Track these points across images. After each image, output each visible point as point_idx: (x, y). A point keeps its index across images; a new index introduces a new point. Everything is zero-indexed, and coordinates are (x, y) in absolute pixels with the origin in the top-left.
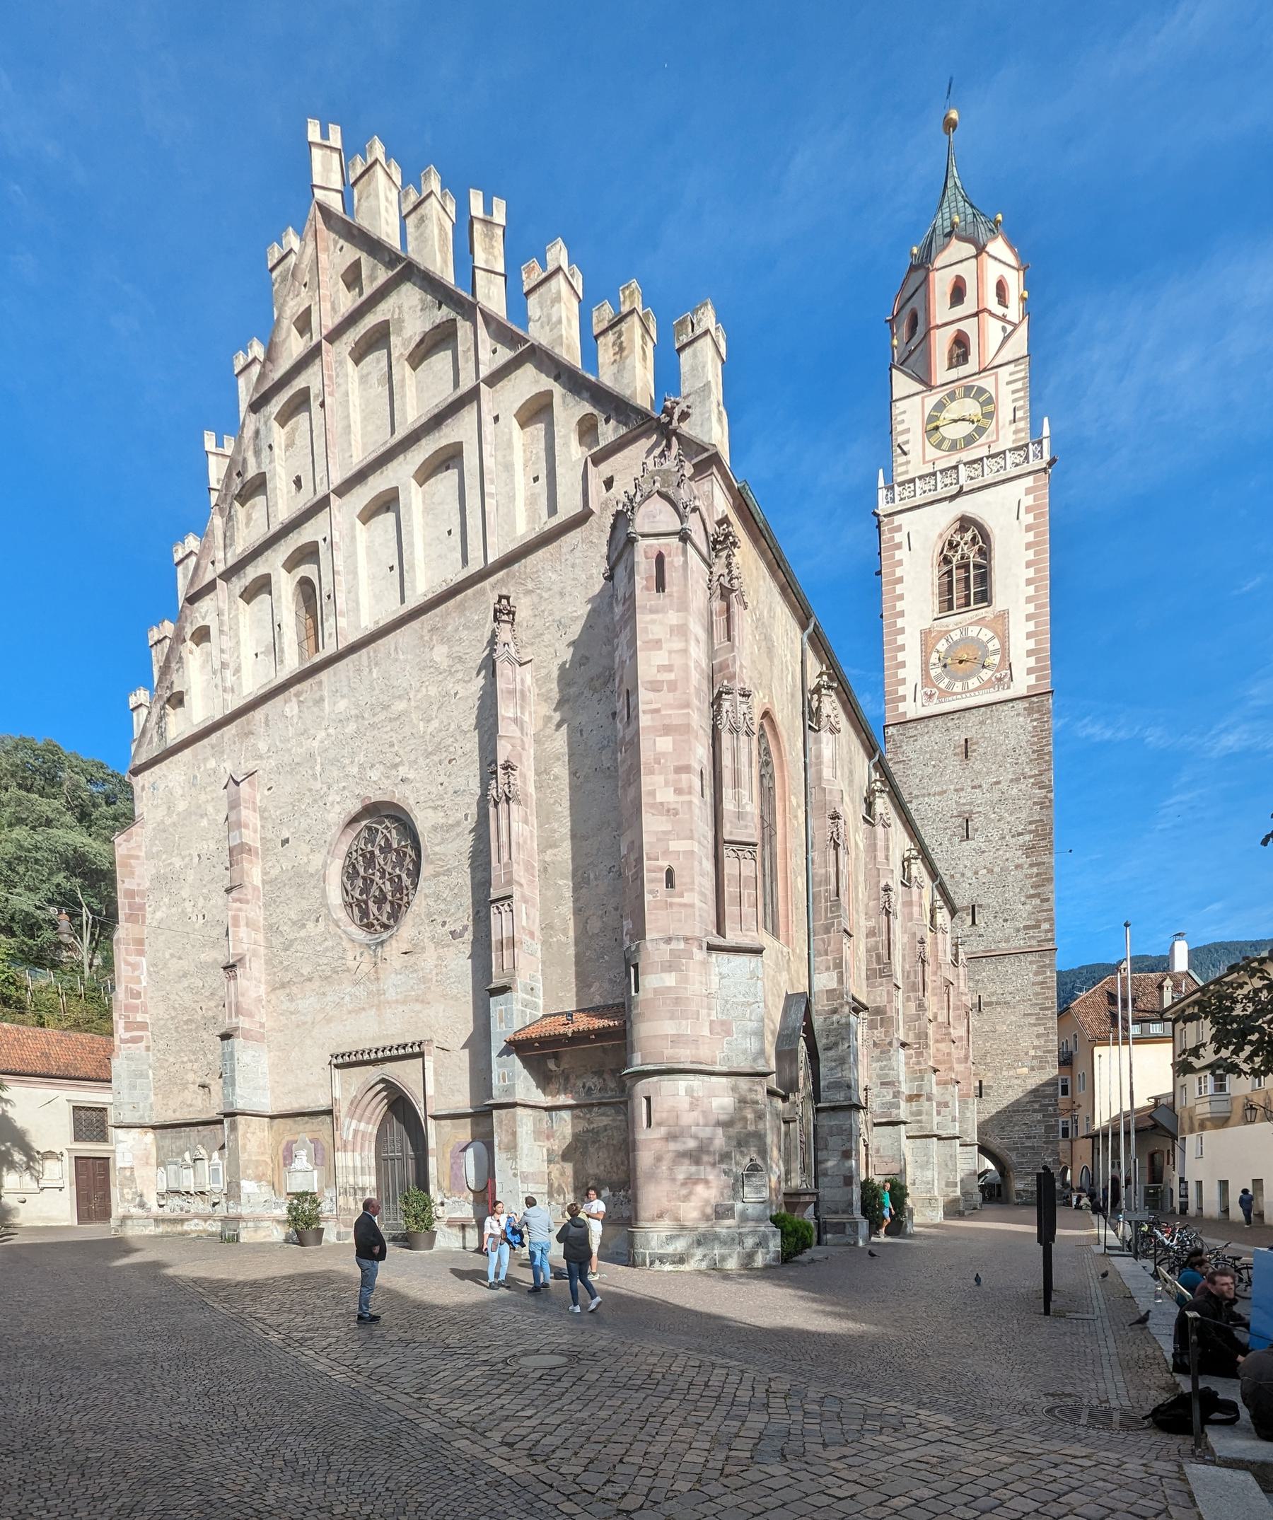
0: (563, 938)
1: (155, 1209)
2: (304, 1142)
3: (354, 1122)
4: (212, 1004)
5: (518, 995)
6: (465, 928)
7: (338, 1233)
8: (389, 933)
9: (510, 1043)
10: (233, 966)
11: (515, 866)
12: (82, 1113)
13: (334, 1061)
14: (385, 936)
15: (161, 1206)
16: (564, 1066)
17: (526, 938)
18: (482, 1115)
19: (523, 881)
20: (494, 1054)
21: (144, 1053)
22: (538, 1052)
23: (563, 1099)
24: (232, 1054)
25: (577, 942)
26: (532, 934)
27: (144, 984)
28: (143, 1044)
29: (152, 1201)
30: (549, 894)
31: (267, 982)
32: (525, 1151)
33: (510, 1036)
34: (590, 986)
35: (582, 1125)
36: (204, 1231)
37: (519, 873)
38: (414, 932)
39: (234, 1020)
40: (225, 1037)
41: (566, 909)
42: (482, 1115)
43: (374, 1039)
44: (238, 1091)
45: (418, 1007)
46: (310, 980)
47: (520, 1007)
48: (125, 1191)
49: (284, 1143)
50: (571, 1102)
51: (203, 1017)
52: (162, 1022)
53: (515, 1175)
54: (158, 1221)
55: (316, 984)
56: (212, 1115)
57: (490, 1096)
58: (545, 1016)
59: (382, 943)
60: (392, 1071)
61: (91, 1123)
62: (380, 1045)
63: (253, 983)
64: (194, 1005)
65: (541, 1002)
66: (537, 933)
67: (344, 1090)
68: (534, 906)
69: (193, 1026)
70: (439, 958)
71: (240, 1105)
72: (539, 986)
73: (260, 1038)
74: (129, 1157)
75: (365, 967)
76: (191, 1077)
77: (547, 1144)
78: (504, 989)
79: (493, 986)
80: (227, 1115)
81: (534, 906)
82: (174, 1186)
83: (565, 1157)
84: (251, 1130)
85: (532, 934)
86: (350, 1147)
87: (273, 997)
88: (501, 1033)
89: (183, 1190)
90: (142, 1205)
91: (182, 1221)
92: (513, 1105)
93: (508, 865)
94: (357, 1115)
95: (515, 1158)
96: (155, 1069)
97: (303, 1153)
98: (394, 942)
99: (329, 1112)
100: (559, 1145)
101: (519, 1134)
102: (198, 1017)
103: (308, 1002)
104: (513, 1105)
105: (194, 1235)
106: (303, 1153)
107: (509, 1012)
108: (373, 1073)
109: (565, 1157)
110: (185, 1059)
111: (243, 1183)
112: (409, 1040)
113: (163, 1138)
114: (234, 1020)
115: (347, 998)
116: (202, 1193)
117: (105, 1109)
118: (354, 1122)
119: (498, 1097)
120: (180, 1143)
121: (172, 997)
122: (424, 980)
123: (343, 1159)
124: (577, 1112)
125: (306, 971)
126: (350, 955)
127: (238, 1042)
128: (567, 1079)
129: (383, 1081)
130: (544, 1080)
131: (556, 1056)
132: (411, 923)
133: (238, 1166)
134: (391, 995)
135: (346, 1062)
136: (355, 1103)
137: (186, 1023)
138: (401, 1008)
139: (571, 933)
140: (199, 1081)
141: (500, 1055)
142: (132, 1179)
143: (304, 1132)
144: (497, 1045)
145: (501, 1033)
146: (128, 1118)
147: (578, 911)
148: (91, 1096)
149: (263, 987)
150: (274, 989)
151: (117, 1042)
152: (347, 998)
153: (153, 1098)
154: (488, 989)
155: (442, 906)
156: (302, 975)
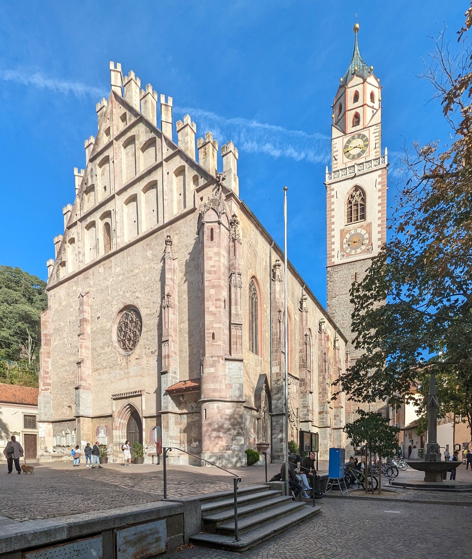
0: (186, 355)
1: (52, 452)
2: (103, 427)
3: (120, 419)
4: (73, 376)
5: (170, 374)
6: (156, 350)
7: (113, 460)
8: (132, 351)
9: (167, 391)
10: (80, 363)
11: (170, 330)
12: (27, 417)
13: (113, 397)
14: (130, 353)
15: (54, 451)
16: (185, 399)
17: (173, 355)
18: (159, 416)
19: (173, 335)
20: (162, 395)
21: (49, 394)
22: (177, 394)
23: (185, 411)
24: (79, 395)
25: (189, 356)
26: (176, 353)
27: (50, 369)
28: (49, 391)
29: (50, 449)
30: (182, 339)
31: (92, 369)
32: (172, 429)
33: (167, 389)
34: (193, 372)
35: (190, 420)
36: (69, 460)
37: (171, 332)
38: (139, 351)
39: (80, 382)
40: (77, 388)
41: (186, 345)
42: (159, 416)
43: (126, 390)
44: (81, 408)
45: (141, 378)
46: (106, 368)
47: (171, 378)
48: (42, 446)
49: (96, 427)
50: (187, 412)
51: (70, 381)
52: (56, 383)
53: (168, 437)
54: (53, 457)
55: (108, 369)
56: (72, 417)
57: (161, 410)
58: (180, 382)
59: (129, 355)
60: (132, 401)
61: (30, 421)
62: (128, 392)
63: (87, 369)
64: (67, 377)
65: (178, 377)
66: (178, 353)
67: (116, 408)
68: (176, 343)
69: (67, 385)
70: (148, 361)
71: (81, 413)
72: (178, 371)
73: (89, 389)
74: (43, 433)
75: (124, 364)
76: (65, 403)
77: (180, 426)
78: (165, 373)
79: (162, 371)
80: (77, 417)
81: (176, 343)
82: (59, 444)
83: (185, 431)
84: (85, 422)
85: (176, 353)
86: (118, 428)
87: (93, 374)
88: (164, 388)
89: (62, 445)
90: (46, 451)
91: (61, 457)
92: (168, 413)
93: (168, 329)
94: (120, 417)
95: (168, 431)
96: (53, 400)
97: (103, 431)
98: (133, 355)
99: (111, 416)
100: (183, 426)
101: (169, 422)
102: (68, 381)
103: (105, 376)
104: (168, 413)
105: (65, 462)
106: (103, 431)
107: (167, 380)
108: (125, 402)
109: (185, 431)
110: (64, 397)
111: (82, 442)
112: (137, 390)
113: (55, 426)
114: (80, 382)
115: (118, 375)
116: (68, 446)
117: (35, 416)
118: (120, 419)
119: (163, 410)
120: (61, 428)
121: (60, 374)
122: (143, 369)
123: (116, 433)
124: (189, 415)
125: (104, 365)
126: (119, 359)
127: (81, 390)
128: (186, 404)
129: (129, 404)
130: (179, 404)
131: (183, 396)
132: (139, 348)
133: (80, 436)
134: (132, 374)
135: (117, 398)
136: (120, 413)
137: (64, 383)
138: (135, 378)
139: (188, 353)
140: (68, 405)
141: (164, 395)
142: (44, 441)
143: (103, 423)
144: (163, 392)
145: (164, 388)
146: (44, 419)
147: (190, 345)
148: (30, 411)
149: (90, 370)
150: (94, 371)
151: (40, 390)
152: (118, 375)
153: (52, 411)
154: (162, 373)
155: (149, 343)
156: (103, 366)
